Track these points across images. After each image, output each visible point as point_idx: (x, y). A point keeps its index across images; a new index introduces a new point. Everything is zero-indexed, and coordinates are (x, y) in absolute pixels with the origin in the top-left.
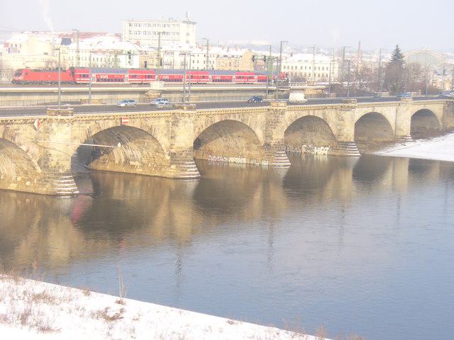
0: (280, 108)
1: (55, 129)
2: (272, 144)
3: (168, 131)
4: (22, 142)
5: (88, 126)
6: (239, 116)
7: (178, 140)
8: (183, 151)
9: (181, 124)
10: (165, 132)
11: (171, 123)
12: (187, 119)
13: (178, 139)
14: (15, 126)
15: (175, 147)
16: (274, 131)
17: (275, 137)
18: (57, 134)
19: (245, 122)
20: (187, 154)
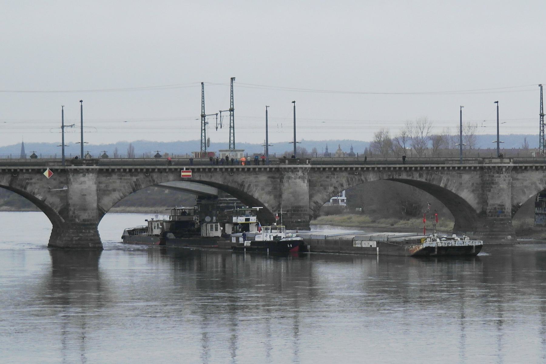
0: (493, 165)
1: (72, 180)
2: (488, 211)
3: (275, 188)
4: (36, 191)
5: (134, 179)
6: (421, 176)
7: (283, 198)
8: (288, 211)
9: (285, 180)
10: (269, 189)
11: (279, 180)
12: (290, 174)
13: (285, 196)
14: (26, 176)
15: (281, 206)
16: (490, 195)
17: (490, 202)
18: (73, 183)
19: (435, 183)
20: (292, 214)
